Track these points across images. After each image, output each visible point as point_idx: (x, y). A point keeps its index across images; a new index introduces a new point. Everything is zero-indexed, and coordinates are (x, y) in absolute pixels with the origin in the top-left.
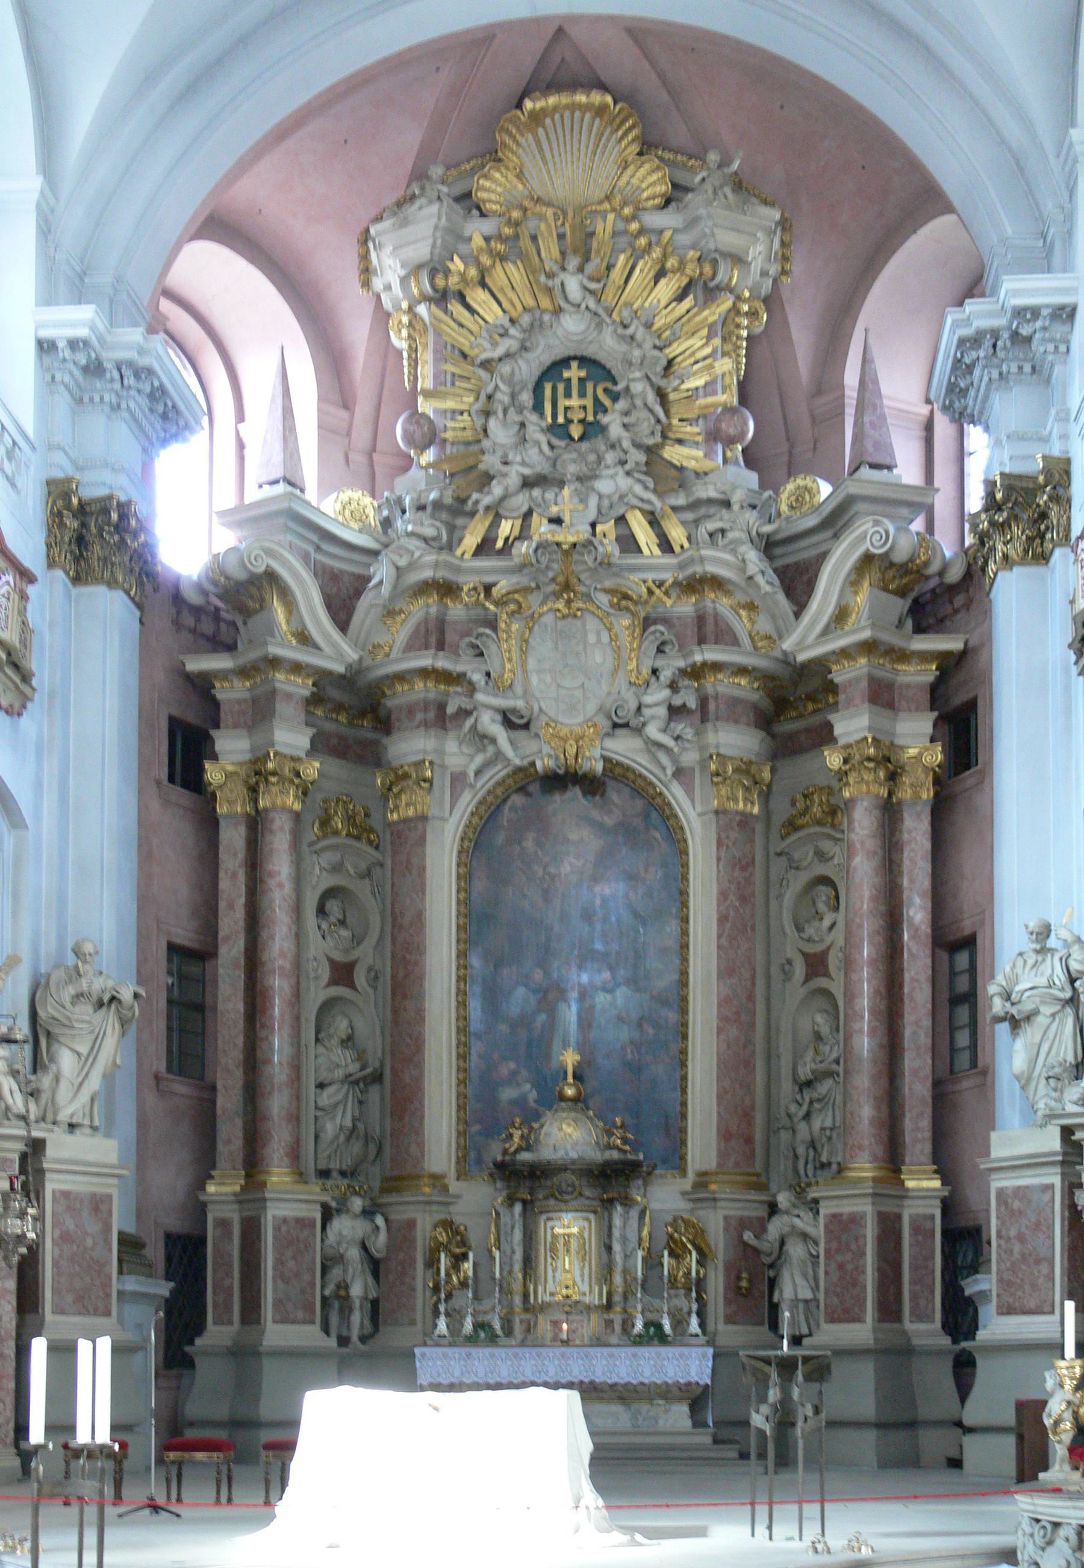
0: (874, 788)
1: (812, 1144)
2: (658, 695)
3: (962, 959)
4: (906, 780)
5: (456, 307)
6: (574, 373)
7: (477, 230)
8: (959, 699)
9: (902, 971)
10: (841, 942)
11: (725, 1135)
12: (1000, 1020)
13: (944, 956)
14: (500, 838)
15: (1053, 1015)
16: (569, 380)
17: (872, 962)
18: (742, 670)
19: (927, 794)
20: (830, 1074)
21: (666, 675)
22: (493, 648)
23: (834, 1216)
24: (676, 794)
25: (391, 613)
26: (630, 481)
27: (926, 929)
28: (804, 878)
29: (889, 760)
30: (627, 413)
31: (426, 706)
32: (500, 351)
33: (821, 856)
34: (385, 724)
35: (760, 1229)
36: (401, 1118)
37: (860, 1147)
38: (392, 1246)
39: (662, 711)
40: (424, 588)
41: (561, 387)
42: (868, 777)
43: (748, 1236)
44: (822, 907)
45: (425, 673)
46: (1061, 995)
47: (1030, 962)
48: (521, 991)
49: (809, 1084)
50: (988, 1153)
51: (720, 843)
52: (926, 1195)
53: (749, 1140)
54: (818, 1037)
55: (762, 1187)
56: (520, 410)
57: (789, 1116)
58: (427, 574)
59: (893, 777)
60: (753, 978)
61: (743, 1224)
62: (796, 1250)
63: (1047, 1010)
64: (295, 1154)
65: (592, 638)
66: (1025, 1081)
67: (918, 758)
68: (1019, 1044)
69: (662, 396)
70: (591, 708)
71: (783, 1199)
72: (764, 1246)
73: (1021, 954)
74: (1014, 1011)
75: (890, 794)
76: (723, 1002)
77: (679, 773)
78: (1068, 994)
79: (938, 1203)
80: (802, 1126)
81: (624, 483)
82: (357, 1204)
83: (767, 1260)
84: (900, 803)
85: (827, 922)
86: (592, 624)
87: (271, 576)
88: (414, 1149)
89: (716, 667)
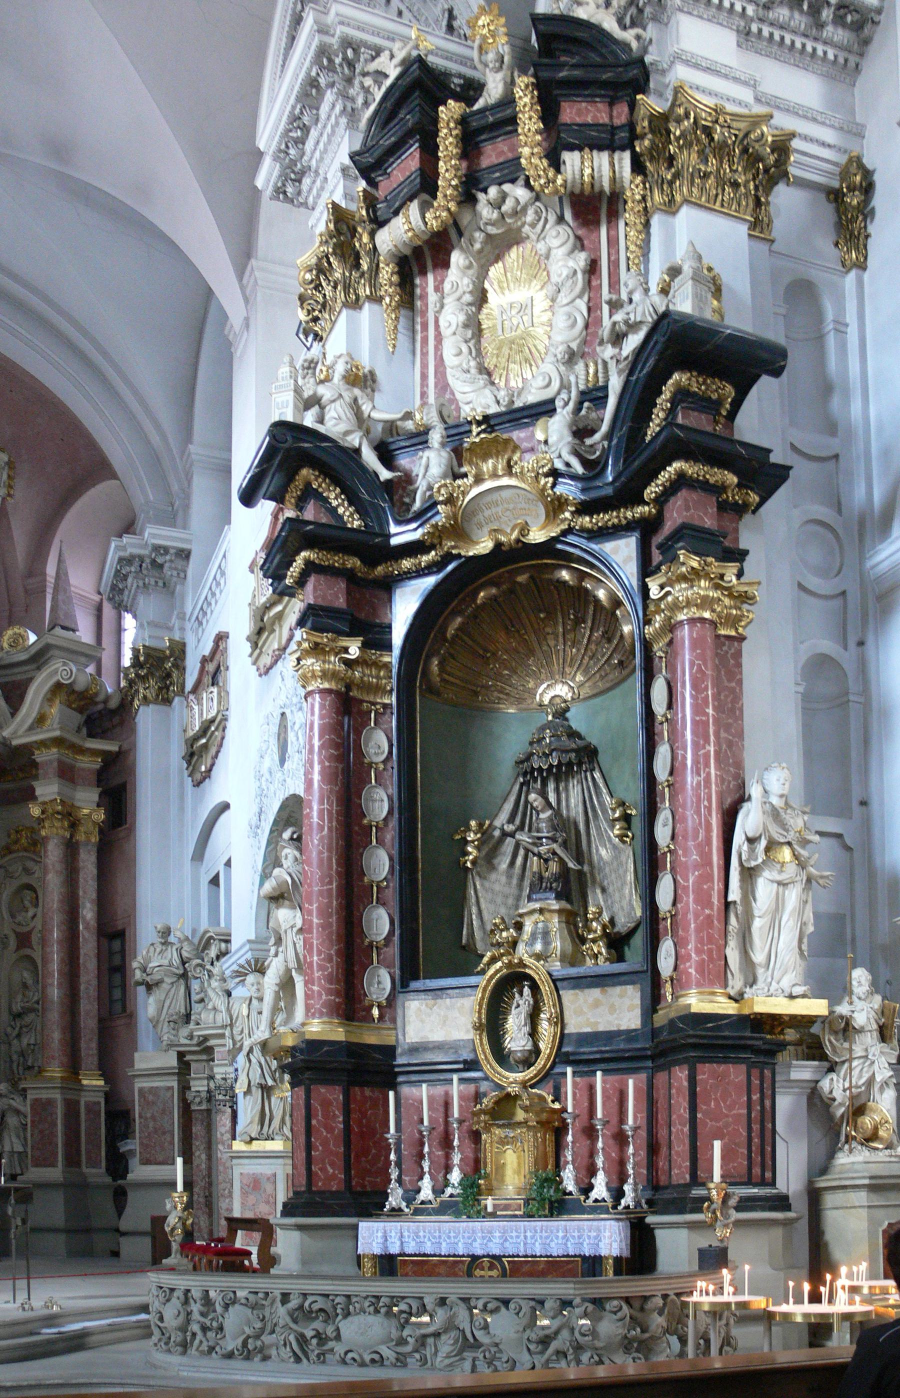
0: (61, 832)
1: (22, 1054)
3: (117, 945)
4: (82, 829)
9: (78, 949)
10: (40, 927)
12: (139, 984)
13: (105, 942)
15: (172, 983)
17: (59, 942)
19: (95, 839)
20: (32, 1010)
23: (36, 1100)
27: (93, 923)
28: (16, 884)
29: (70, 815)
33: (27, 871)
37: (53, 1057)
44: (27, 903)
46: (177, 971)
47: (158, 950)
49: (19, 1015)
54: (25, 986)
57: (7, 1035)
59: (74, 825)
63: (168, 980)
66: (155, 1023)
67: (89, 815)
68: (151, 1000)
73: (152, 944)
74: (148, 979)
75: (72, 836)
78: (181, 971)
79: (102, 1094)
80: (15, 1042)
84: (77, 842)
85: (30, 914)
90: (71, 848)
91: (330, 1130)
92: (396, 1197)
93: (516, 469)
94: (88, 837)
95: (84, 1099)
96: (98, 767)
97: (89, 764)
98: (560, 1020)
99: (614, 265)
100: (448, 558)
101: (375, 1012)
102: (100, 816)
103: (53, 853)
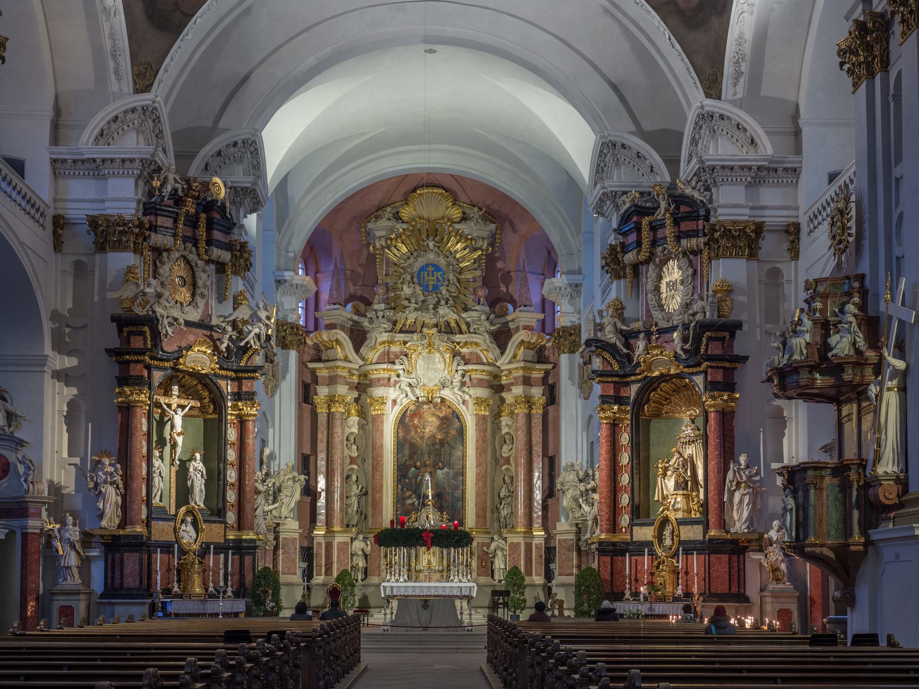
0: (525, 411)
2: (458, 377)
5: (393, 248)
6: (431, 269)
7: (400, 227)
8: (550, 382)
11: (478, 516)
14: (407, 421)
16: (428, 271)
18: (484, 371)
19: (541, 412)
21: (460, 372)
22: (406, 362)
24: (462, 408)
25: (373, 348)
26: (449, 310)
30: (447, 286)
31: (384, 379)
32: (407, 264)
34: (371, 384)
35: (488, 545)
36: (375, 510)
38: (372, 551)
39: (459, 384)
40: (384, 343)
41: (426, 273)
42: (523, 407)
43: (485, 548)
45: (384, 370)
48: (413, 469)
50: (555, 529)
51: (476, 425)
52: (539, 536)
53: (485, 518)
55: (489, 533)
56: (414, 283)
58: (385, 339)
60: (487, 467)
61: (484, 544)
62: (499, 553)
64: (342, 521)
65: (437, 360)
69: (459, 280)
70: (437, 381)
71: (496, 537)
72: (490, 552)
75: (530, 411)
76: (477, 475)
77: (464, 402)
81: (447, 311)
82: (361, 537)
83: (491, 556)
86: (437, 355)
87: (337, 341)
88: (379, 520)
89: (476, 370)
90: (529, 417)
91: (606, 571)
92: (627, 595)
93: (664, 354)
94: (537, 411)
95: (535, 541)
96: (542, 376)
97: (537, 375)
98: (679, 536)
99: (702, 271)
100: (646, 377)
101: (624, 530)
102: (543, 400)
103: (521, 421)
